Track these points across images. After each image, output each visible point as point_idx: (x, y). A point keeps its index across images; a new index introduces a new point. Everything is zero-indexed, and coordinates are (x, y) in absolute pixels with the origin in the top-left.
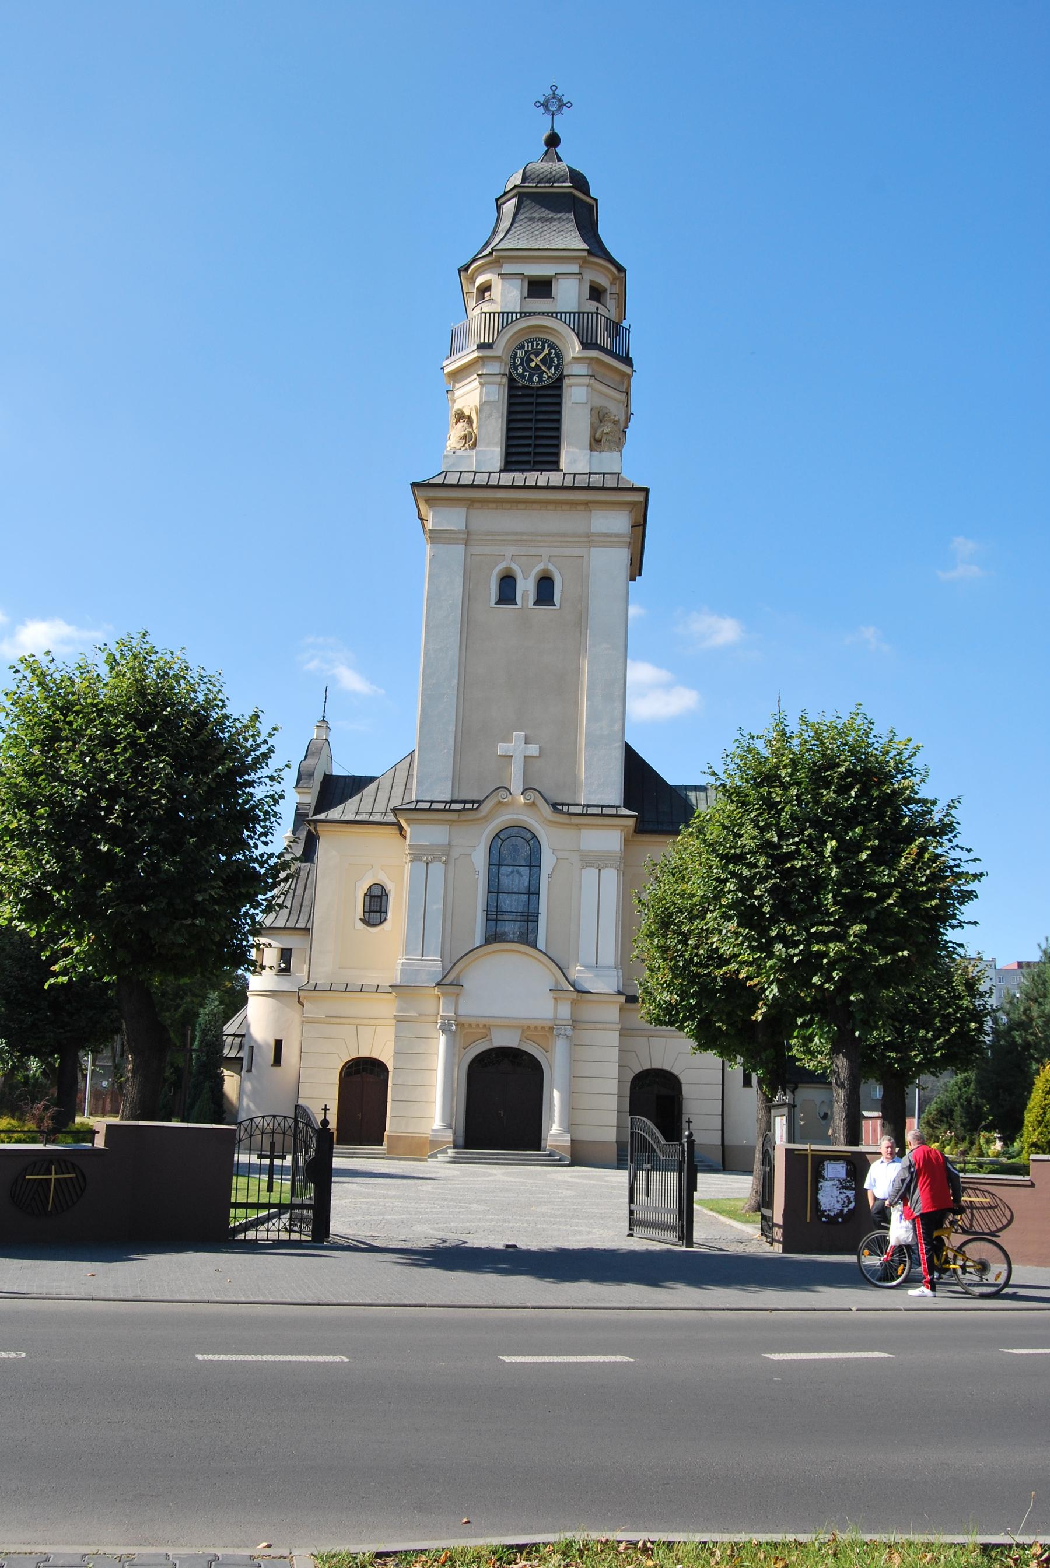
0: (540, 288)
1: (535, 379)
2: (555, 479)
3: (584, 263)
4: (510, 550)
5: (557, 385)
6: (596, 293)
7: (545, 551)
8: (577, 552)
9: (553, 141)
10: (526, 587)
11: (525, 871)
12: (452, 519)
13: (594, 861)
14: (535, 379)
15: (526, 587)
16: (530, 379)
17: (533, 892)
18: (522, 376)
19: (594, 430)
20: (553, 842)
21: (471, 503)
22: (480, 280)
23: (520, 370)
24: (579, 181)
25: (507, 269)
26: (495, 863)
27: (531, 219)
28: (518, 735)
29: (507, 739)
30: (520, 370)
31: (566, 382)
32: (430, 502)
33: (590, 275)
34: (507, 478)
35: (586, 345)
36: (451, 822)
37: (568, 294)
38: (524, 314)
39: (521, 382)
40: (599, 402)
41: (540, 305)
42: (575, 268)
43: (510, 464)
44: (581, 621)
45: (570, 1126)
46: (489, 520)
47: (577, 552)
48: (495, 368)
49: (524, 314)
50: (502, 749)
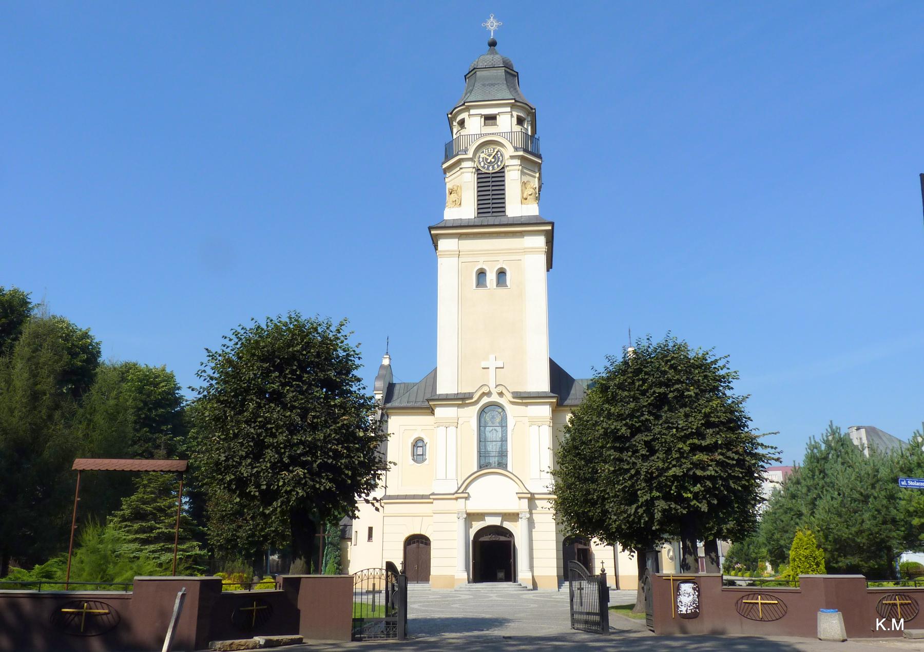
0: (490, 119)
1: (491, 168)
4: (482, 259)
5: (501, 173)
10: (491, 277)
11: (499, 429)
13: (533, 422)
14: (491, 168)
15: (491, 277)
16: (488, 169)
17: (504, 440)
18: (484, 167)
19: (523, 193)
20: (513, 412)
21: (460, 236)
22: (459, 118)
23: (482, 164)
25: (472, 112)
26: (481, 425)
27: (484, 85)
28: (492, 357)
30: (482, 164)
31: (506, 169)
33: (515, 114)
34: (478, 222)
35: (516, 149)
39: (484, 171)
42: (508, 109)
49: (481, 135)
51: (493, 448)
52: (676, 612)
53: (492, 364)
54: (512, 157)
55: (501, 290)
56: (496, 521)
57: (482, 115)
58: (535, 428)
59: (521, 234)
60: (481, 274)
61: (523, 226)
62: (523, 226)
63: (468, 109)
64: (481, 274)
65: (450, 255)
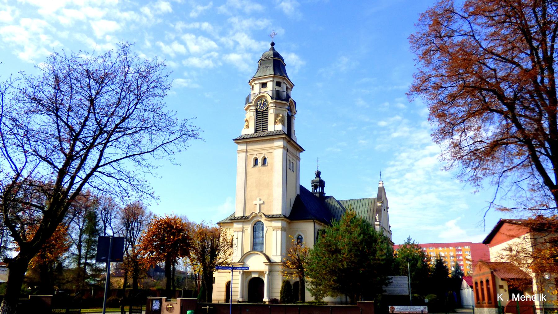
0: (264, 85)
2: (266, 133)
3: (274, 77)
6: (278, 84)
7: (264, 152)
8: (271, 151)
9: (273, 44)
10: (260, 161)
12: (243, 147)
15: (260, 161)
19: (275, 119)
20: (267, 224)
21: (247, 142)
24: (276, 55)
25: (256, 82)
26: (254, 230)
27: (263, 68)
28: (258, 199)
29: (256, 200)
32: (237, 143)
35: (272, 98)
36: (243, 222)
37: (270, 86)
38: (260, 93)
40: (277, 112)
41: (263, 90)
43: (256, 131)
44: (272, 169)
45: (269, 296)
46: (250, 147)
47: (271, 151)
48: (252, 108)
49: (260, 93)
50: (255, 202)
51: (258, 241)
52: (152, 308)
53: (258, 202)
54: (271, 103)
55: (264, 168)
56: (256, 276)
57: (260, 83)
58: (275, 231)
59: (273, 140)
60: (256, 160)
61: (274, 136)
62: (274, 136)
63: (254, 80)
64: (256, 160)
65: (243, 152)
